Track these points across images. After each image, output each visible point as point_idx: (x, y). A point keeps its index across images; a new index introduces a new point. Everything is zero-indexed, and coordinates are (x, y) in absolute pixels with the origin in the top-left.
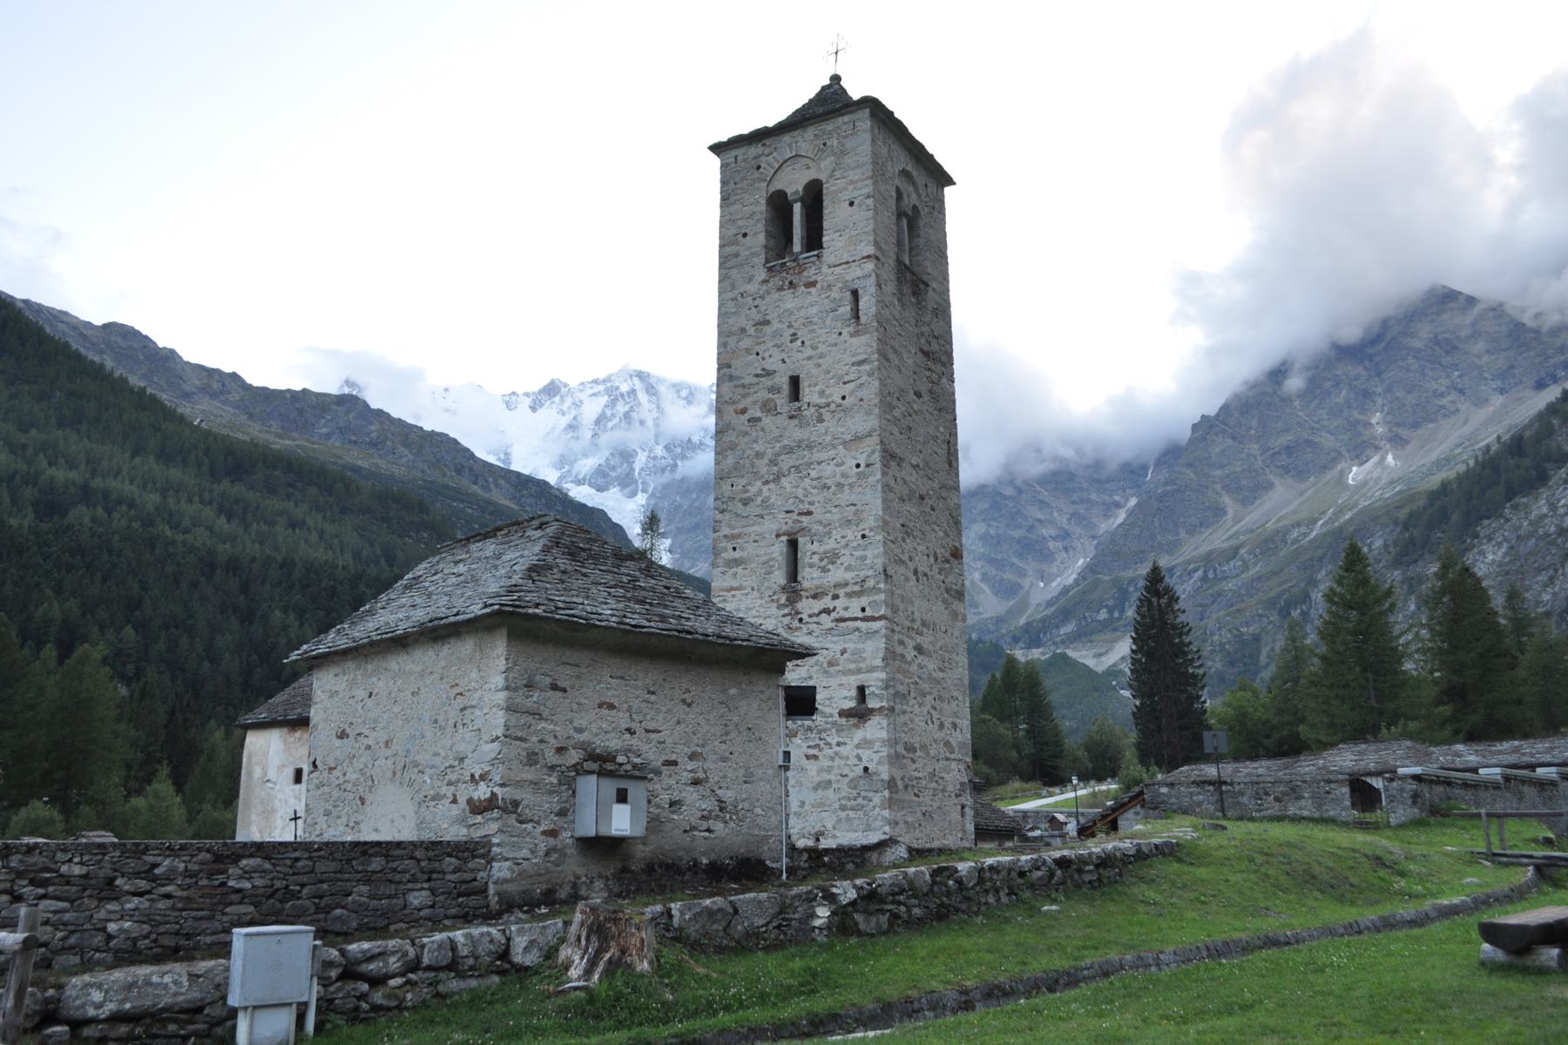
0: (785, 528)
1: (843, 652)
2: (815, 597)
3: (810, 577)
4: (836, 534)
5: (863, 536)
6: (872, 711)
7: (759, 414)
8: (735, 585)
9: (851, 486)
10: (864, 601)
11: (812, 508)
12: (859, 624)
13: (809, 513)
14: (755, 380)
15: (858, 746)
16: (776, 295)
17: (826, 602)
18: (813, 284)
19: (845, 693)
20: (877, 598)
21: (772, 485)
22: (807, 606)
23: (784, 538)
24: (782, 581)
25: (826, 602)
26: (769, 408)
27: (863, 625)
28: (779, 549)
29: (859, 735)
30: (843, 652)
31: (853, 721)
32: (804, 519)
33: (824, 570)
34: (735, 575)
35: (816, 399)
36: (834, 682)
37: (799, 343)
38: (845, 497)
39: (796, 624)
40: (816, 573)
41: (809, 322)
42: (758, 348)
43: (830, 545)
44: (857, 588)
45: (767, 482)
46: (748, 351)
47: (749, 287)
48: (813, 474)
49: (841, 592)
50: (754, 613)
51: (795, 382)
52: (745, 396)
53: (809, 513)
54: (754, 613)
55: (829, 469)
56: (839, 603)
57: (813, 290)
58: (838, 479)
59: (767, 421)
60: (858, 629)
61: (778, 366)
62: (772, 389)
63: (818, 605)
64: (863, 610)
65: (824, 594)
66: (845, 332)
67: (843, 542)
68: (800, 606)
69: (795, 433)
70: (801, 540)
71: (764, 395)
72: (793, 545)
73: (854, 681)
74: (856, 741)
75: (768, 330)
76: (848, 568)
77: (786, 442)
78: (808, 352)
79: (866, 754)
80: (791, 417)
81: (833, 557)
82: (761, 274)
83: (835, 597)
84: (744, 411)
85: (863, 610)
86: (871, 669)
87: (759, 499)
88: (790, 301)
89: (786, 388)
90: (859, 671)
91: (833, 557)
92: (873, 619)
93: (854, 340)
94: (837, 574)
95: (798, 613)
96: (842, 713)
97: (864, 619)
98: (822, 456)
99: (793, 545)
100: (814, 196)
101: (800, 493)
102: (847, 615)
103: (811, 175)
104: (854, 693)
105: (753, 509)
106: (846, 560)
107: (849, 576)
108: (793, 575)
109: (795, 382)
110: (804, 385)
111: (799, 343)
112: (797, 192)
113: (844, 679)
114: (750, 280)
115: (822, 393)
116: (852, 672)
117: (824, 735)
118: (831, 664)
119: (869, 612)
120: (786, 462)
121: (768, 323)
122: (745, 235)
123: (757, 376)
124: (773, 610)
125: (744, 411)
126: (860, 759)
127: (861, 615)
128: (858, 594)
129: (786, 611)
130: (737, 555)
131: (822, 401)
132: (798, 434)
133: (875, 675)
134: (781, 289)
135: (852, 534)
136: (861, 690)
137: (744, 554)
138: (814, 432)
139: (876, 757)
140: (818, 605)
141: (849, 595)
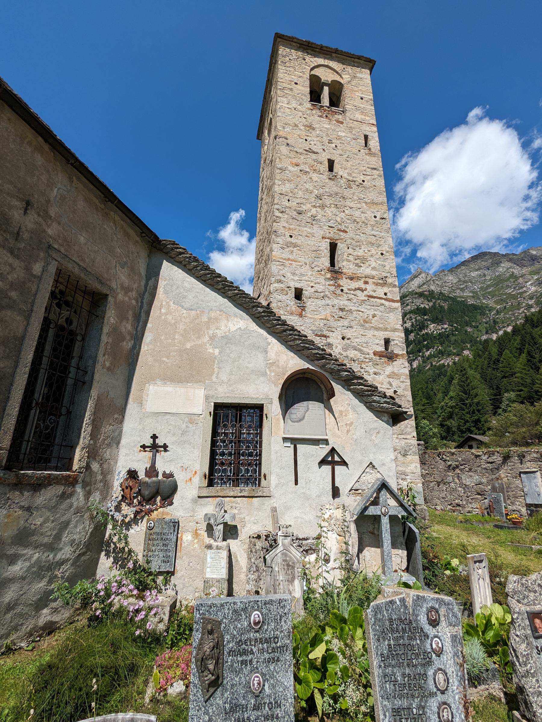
0: (328, 235)
1: (374, 316)
2: (351, 279)
5: (382, 254)
6: (397, 355)
7: (308, 170)
8: (291, 257)
9: (373, 226)
10: (386, 289)
11: (346, 229)
12: (383, 301)
13: (346, 232)
14: (304, 152)
15: (389, 376)
17: (360, 284)
18: (342, 123)
19: (377, 341)
20: (394, 289)
21: (318, 209)
23: (329, 241)
24: (327, 264)
25: (360, 284)
27: (387, 303)
28: (325, 246)
29: (389, 369)
30: (374, 316)
31: (384, 360)
32: (341, 233)
33: (357, 265)
34: (292, 252)
35: (345, 175)
36: (370, 333)
38: (368, 230)
39: (338, 292)
40: (352, 266)
42: (307, 138)
43: (360, 253)
44: (380, 281)
45: (315, 206)
48: (347, 212)
49: (370, 281)
50: (306, 278)
51: (331, 164)
53: (346, 232)
54: (306, 278)
56: (370, 287)
57: (341, 125)
58: (363, 219)
60: (383, 305)
64: (386, 294)
65: (358, 278)
66: (362, 151)
67: (370, 254)
68: (341, 282)
69: (332, 187)
70: (340, 246)
72: (333, 247)
73: (384, 335)
74: (387, 373)
76: (374, 269)
77: (327, 190)
78: (341, 152)
79: (395, 383)
80: (330, 179)
81: (364, 260)
82: (309, 105)
83: (366, 283)
85: (386, 294)
86: (395, 330)
87: (309, 214)
88: (325, 124)
90: (386, 330)
91: (364, 260)
92: (393, 301)
94: (365, 270)
95: (339, 286)
96: (375, 354)
97: (386, 300)
98: (351, 205)
99: (333, 247)
101: (339, 219)
102: (374, 294)
104: (383, 342)
107: (374, 273)
111: (334, 145)
112: (327, 81)
113: (376, 333)
116: (378, 329)
117: (363, 366)
118: (365, 321)
119: (389, 296)
122: (296, 84)
123: (306, 150)
124: (322, 280)
126: (391, 385)
127: (385, 297)
128: (384, 284)
129: (332, 282)
130: (293, 240)
131: (351, 178)
132: (335, 189)
133: (397, 334)
134: (321, 116)
136: (387, 342)
137: (299, 242)
138: (347, 193)
139: (403, 385)
140: (354, 285)
141: (377, 284)
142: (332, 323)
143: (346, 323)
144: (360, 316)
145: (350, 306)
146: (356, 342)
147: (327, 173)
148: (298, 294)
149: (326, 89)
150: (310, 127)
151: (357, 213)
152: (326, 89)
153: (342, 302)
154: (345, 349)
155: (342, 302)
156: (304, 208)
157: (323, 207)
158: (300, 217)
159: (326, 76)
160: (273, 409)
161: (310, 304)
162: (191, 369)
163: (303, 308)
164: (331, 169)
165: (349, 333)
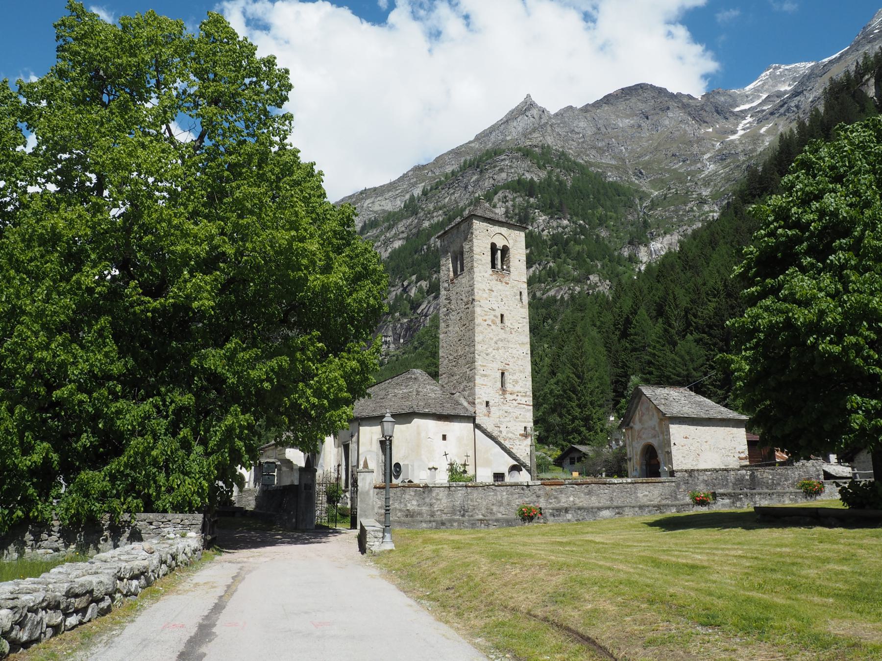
3: (509, 387)
4: (518, 374)
17: (514, 397)
22: (508, 396)
25: (514, 397)
26: (494, 322)
35: (509, 325)
36: (518, 424)
38: (520, 363)
41: (506, 296)
43: (515, 377)
46: (486, 299)
47: (485, 275)
55: (515, 351)
59: (493, 327)
61: (496, 308)
62: (495, 316)
63: (512, 397)
69: (502, 334)
71: (492, 317)
72: (503, 374)
73: (524, 425)
75: (494, 294)
81: (517, 382)
82: (490, 271)
88: (500, 286)
94: (517, 388)
99: (503, 374)
100: (505, 250)
103: (505, 243)
105: (490, 358)
106: (520, 383)
107: (521, 389)
108: (503, 384)
109: (502, 316)
110: (505, 318)
116: (522, 422)
120: (500, 344)
128: (525, 396)
130: (484, 373)
132: (504, 336)
135: (522, 376)
136: (525, 428)
140: (512, 397)
142: (502, 419)
143: (507, 419)
144: (514, 415)
145: (510, 410)
146: (512, 429)
148: (487, 403)
149: (499, 252)
151: (515, 351)
152: (499, 252)
153: (506, 408)
154: (507, 433)
155: (506, 408)
156: (490, 350)
157: (498, 349)
158: (487, 357)
159: (500, 244)
160: (507, 474)
161: (493, 409)
162: (488, 463)
163: (489, 412)
164: (502, 321)
165: (509, 425)
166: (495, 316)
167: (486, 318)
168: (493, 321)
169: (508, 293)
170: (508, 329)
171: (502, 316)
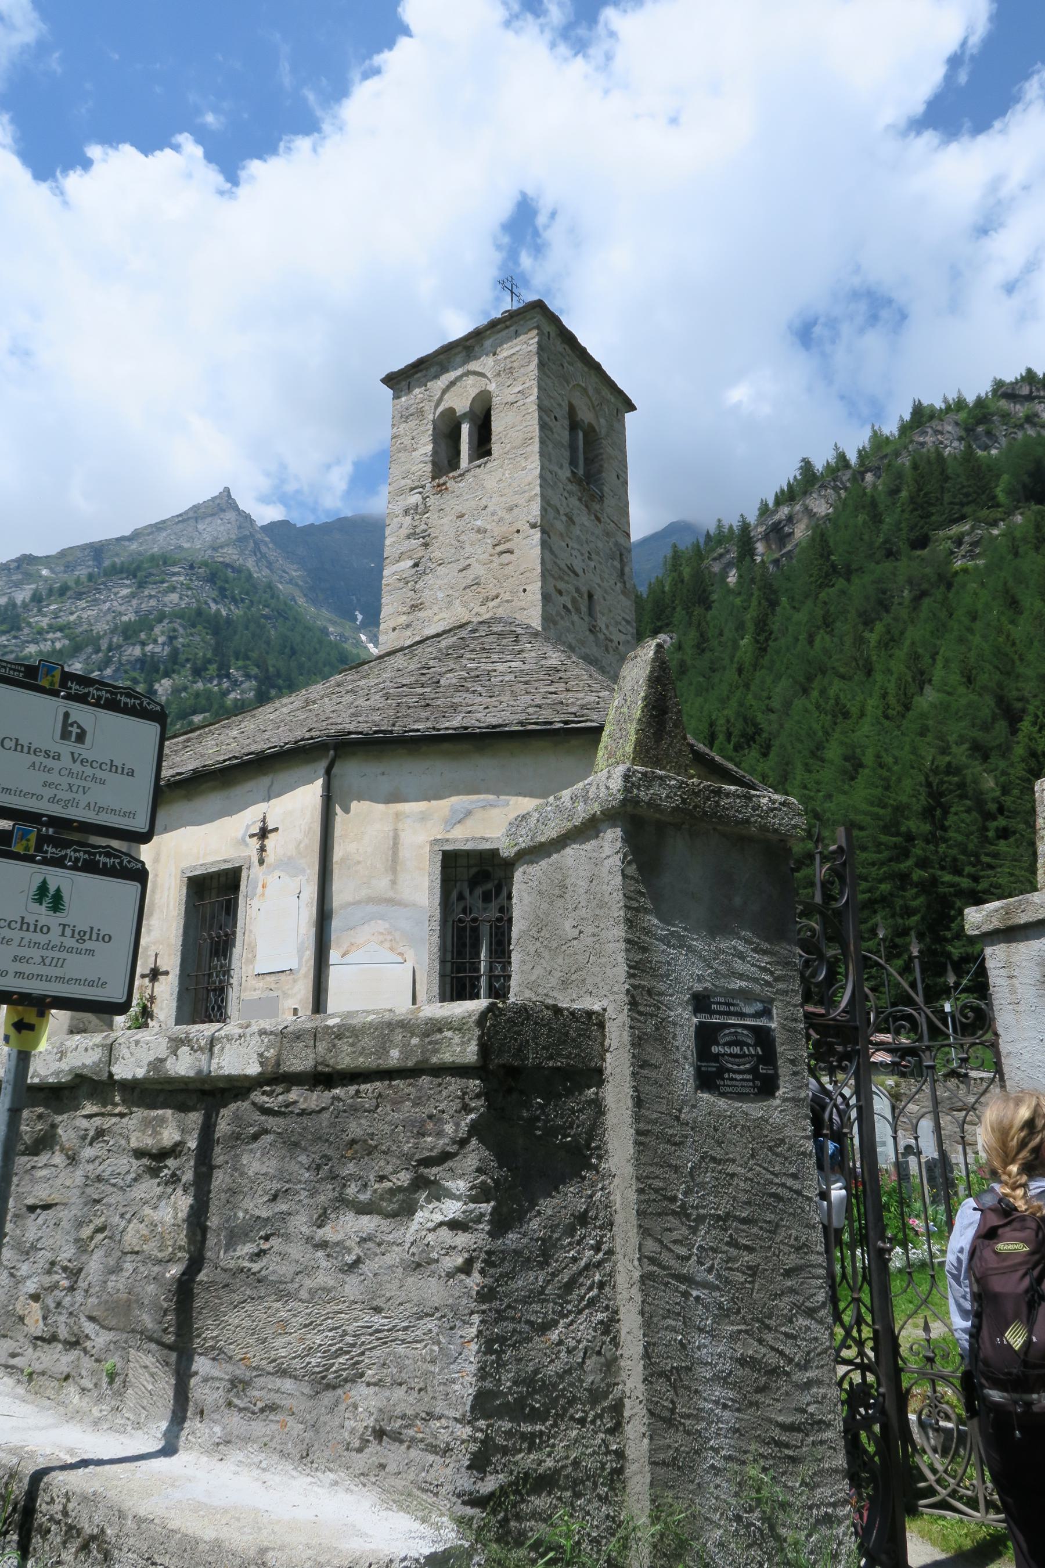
16: (578, 503)
35: (603, 627)
37: (592, 564)
47: (560, 472)
52: (562, 579)
59: (575, 618)
62: (578, 590)
78: (599, 581)
84: (560, 593)
88: (584, 519)
89: (586, 596)
93: (622, 597)
114: (561, 467)
115: (607, 627)
121: (574, 523)
125: (560, 593)
134: (580, 500)
147: (586, 618)
150: (571, 520)
159: (585, 415)
166: (578, 590)
167: (561, 585)
168: (574, 601)
169: (600, 545)
170: (601, 636)
171: (590, 596)
